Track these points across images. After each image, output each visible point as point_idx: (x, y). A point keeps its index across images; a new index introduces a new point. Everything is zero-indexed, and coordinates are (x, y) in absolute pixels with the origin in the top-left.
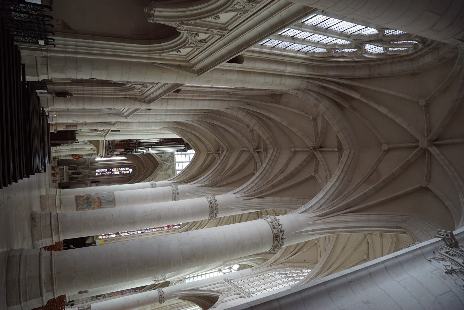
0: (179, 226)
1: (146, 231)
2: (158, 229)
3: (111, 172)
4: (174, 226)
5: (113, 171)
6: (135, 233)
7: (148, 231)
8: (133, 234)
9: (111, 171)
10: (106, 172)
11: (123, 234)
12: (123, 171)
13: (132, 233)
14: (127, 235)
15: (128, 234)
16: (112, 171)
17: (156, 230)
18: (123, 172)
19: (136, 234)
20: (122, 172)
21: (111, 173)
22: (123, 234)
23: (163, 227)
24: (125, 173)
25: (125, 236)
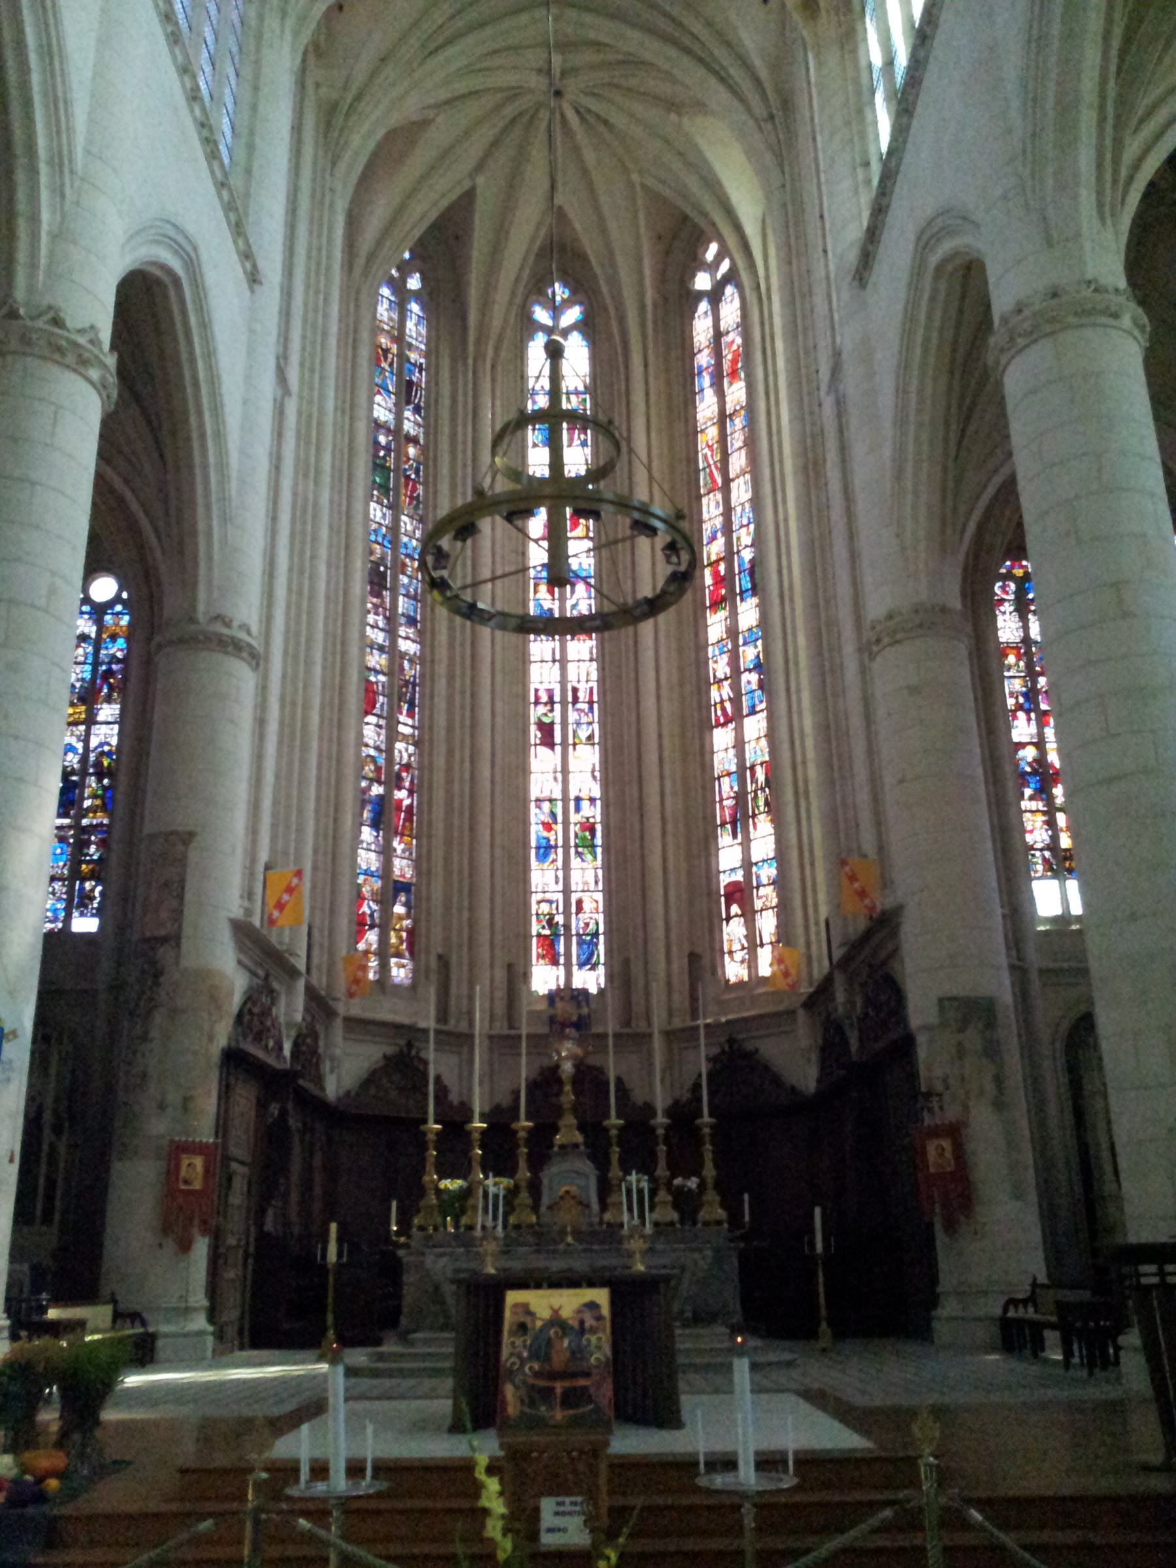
0: (729, 290)
1: (747, 555)
2: (738, 461)
3: (92, 781)
4: (718, 335)
5: (84, 759)
6: (749, 654)
7: (747, 540)
8: (758, 667)
9: (81, 785)
10: (77, 826)
11: (758, 752)
12: (96, 664)
13: (754, 677)
14: (770, 719)
15: (753, 712)
16: (83, 773)
17: (743, 473)
18: (113, 659)
19: (765, 638)
20: (109, 673)
21: (100, 776)
22: (749, 758)
23: (723, 418)
24: (121, 643)
25: (771, 735)
